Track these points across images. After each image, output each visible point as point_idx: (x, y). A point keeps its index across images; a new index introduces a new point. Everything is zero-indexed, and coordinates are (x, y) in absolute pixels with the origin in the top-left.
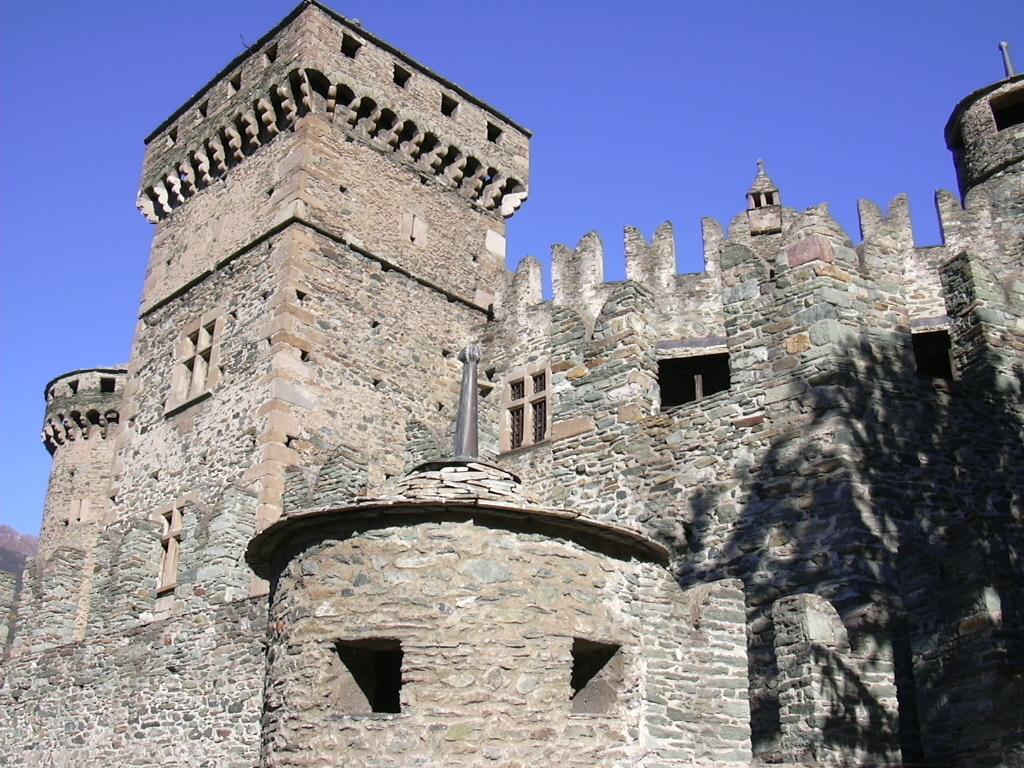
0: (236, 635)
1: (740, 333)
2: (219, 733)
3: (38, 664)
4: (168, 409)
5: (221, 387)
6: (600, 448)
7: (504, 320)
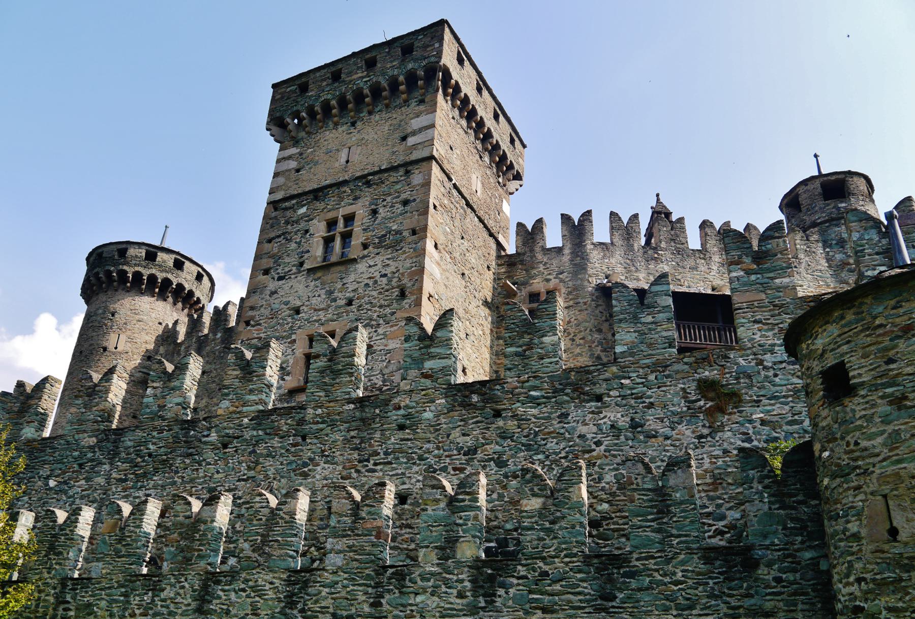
0: (467, 405)
1: (867, 257)
2: (455, 469)
3: (250, 420)
4: (307, 266)
5: (364, 257)
6: (770, 310)
7: (524, 254)
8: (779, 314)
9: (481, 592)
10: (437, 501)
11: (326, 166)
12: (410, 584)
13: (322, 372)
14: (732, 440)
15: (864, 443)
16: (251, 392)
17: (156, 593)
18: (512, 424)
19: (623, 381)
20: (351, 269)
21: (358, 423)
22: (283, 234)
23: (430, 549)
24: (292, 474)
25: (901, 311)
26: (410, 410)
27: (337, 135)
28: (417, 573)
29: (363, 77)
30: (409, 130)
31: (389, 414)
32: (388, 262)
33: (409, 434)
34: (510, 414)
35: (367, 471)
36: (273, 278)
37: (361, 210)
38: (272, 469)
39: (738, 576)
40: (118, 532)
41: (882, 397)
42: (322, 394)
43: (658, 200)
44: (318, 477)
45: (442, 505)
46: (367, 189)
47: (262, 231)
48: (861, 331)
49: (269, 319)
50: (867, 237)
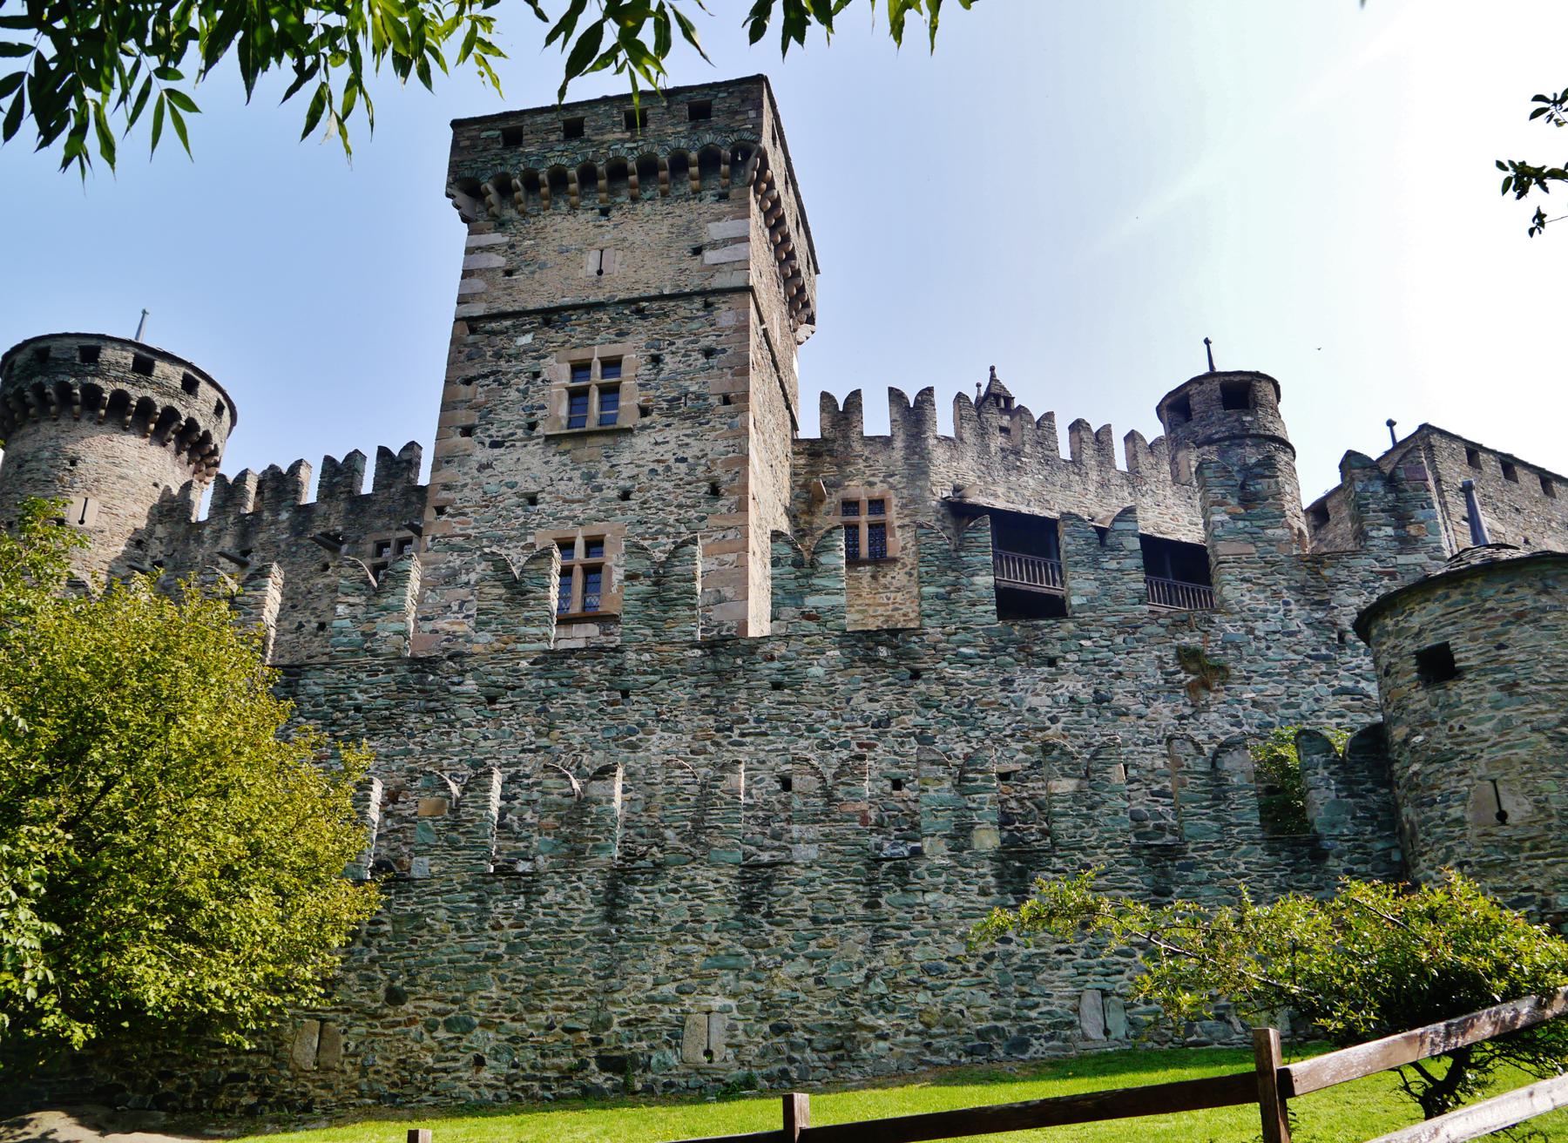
5: (644, 428)
7: (834, 441)
8: (1272, 573)
9: (1010, 888)
10: (940, 780)
11: (562, 272)
12: (916, 880)
13: (644, 600)
14: (1219, 724)
15: (1470, 728)
16: (528, 621)
17: (533, 897)
18: (937, 690)
19: (1083, 642)
20: (624, 444)
21: (710, 677)
22: (493, 373)
23: (936, 838)
24: (612, 745)
25: (1514, 596)
26: (789, 663)
27: (576, 226)
28: (924, 867)
29: (624, 141)
30: (706, 240)
31: (758, 666)
32: (687, 440)
33: (790, 695)
34: (934, 676)
35: (730, 743)
36: (483, 443)
37: (633, 353)
38: (577, 735)
39: (1306, 867)
40: (446, 814)
41: (1491, 683)
42: (649, 632)
43: (993, 376)
44: (654, 749)
45: (947, 785)
46: (639, 322)
47: (451, 363)
48: (1470, 613)
49: (482, 507)
50: (1371, 489)
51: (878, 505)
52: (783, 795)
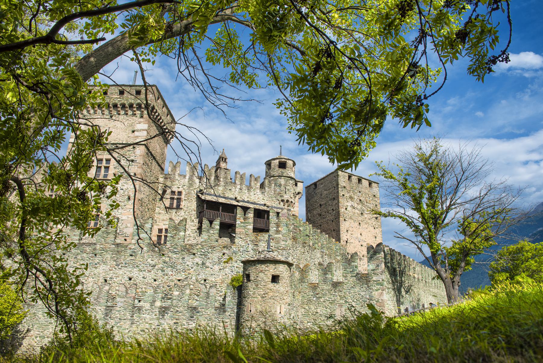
18: (167, 259)
30: (136, 129)
42: (103, 240)
51: (180, 193)
52: (129, 282)
